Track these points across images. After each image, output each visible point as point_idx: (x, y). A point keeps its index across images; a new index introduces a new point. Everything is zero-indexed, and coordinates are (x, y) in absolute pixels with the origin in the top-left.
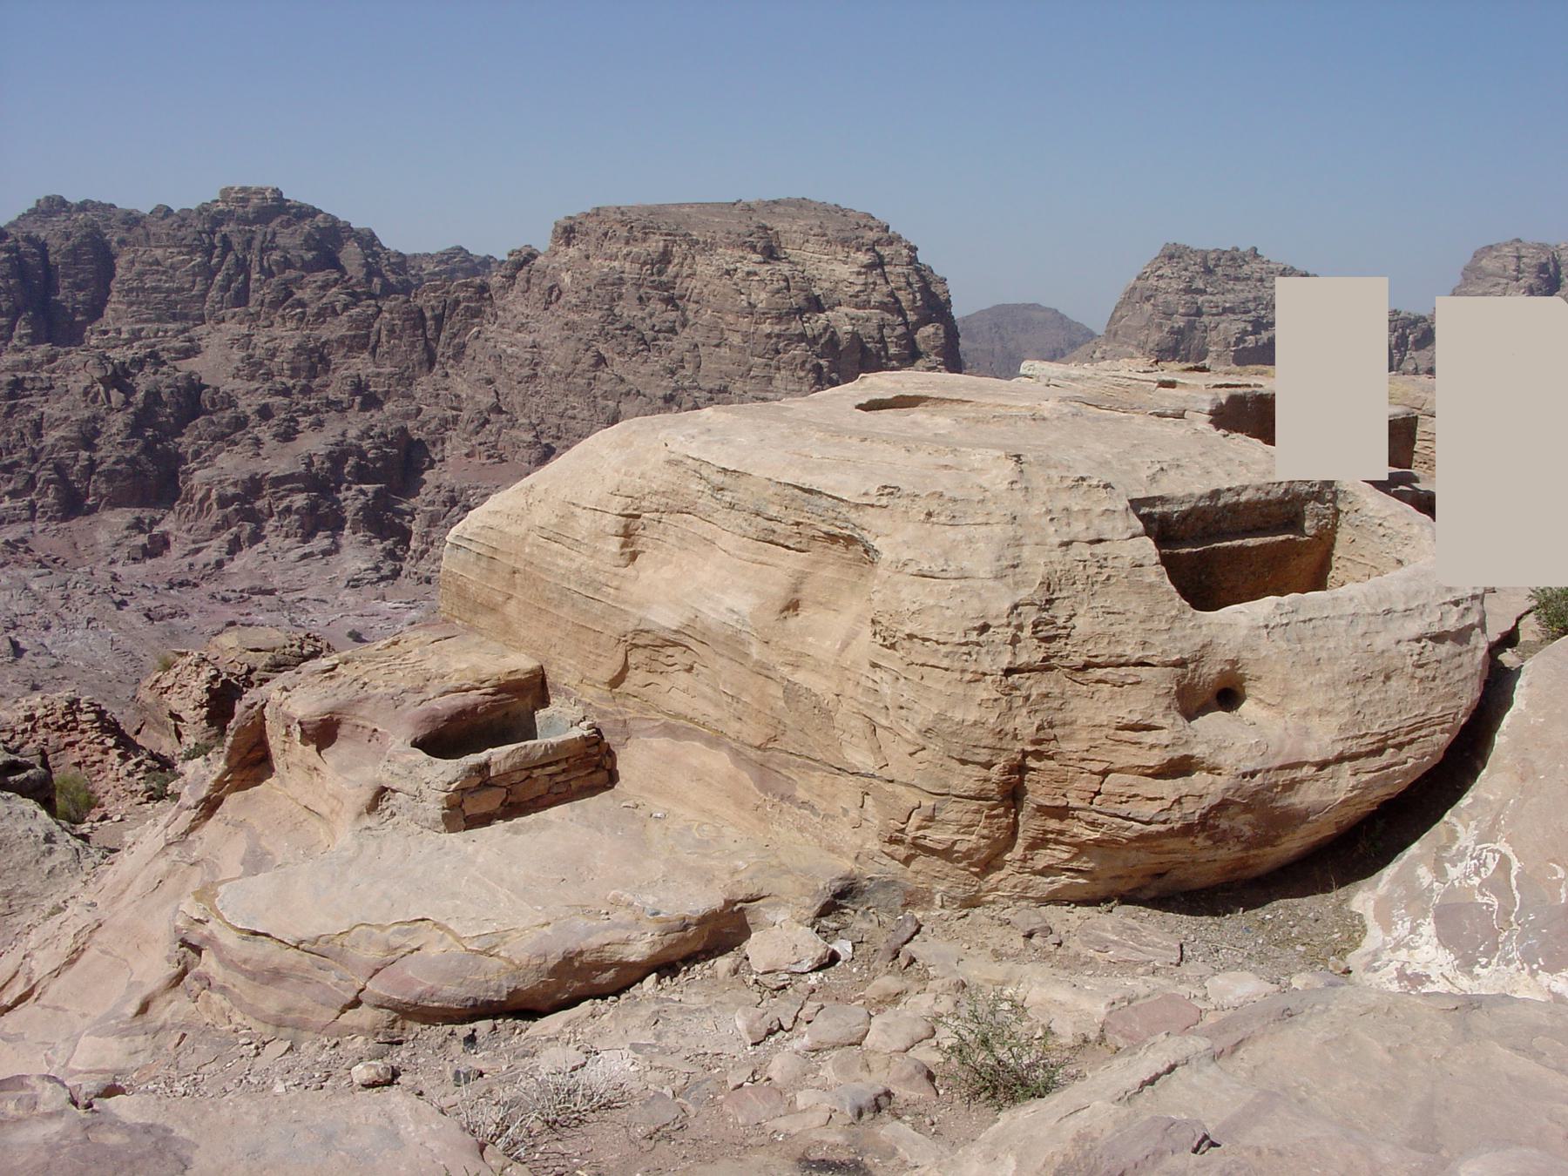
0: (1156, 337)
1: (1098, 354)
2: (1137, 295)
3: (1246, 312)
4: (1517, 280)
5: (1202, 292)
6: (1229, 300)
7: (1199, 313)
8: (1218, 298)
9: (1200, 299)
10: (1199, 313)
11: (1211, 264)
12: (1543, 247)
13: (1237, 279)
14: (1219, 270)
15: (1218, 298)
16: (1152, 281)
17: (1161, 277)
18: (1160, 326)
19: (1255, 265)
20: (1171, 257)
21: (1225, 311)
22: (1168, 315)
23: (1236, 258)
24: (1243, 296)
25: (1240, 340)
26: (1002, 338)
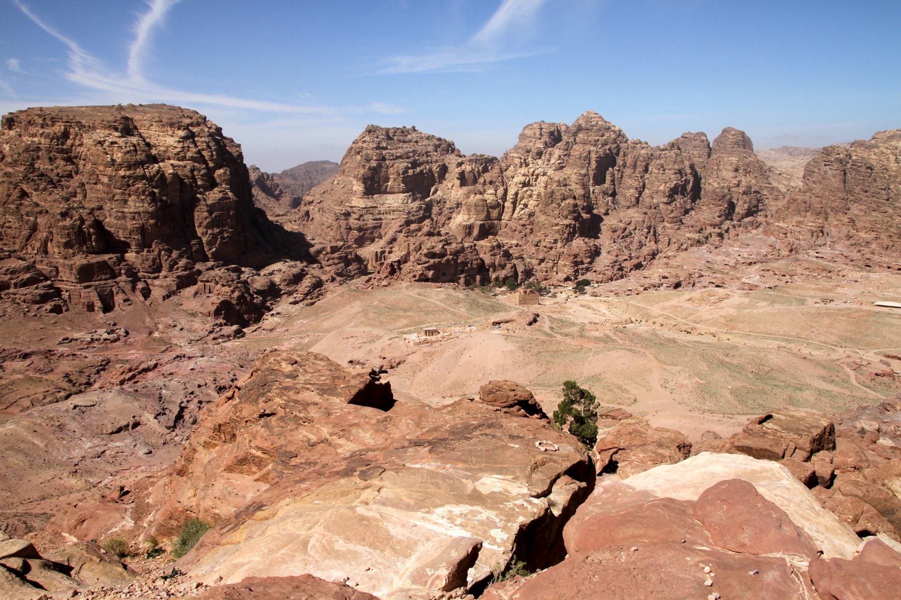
0: (362, 171)
2: (354, 151)
5: (386, 148)
6: (400, 152)
7: (384, 159)
8: (394, 151)
9: (384, 152)
10: (384, 159)
11: (391, 135)
12: (553, 124)
13: (404, 142)
14: (395, 138)
15: (394, 151)
16: (360, 144)
17: (364, 142)
18: (364, 166)
20: (370, 132)
21: (397, 158)
22: (368, 160)
23: (404, 132)
25: (405, 172)
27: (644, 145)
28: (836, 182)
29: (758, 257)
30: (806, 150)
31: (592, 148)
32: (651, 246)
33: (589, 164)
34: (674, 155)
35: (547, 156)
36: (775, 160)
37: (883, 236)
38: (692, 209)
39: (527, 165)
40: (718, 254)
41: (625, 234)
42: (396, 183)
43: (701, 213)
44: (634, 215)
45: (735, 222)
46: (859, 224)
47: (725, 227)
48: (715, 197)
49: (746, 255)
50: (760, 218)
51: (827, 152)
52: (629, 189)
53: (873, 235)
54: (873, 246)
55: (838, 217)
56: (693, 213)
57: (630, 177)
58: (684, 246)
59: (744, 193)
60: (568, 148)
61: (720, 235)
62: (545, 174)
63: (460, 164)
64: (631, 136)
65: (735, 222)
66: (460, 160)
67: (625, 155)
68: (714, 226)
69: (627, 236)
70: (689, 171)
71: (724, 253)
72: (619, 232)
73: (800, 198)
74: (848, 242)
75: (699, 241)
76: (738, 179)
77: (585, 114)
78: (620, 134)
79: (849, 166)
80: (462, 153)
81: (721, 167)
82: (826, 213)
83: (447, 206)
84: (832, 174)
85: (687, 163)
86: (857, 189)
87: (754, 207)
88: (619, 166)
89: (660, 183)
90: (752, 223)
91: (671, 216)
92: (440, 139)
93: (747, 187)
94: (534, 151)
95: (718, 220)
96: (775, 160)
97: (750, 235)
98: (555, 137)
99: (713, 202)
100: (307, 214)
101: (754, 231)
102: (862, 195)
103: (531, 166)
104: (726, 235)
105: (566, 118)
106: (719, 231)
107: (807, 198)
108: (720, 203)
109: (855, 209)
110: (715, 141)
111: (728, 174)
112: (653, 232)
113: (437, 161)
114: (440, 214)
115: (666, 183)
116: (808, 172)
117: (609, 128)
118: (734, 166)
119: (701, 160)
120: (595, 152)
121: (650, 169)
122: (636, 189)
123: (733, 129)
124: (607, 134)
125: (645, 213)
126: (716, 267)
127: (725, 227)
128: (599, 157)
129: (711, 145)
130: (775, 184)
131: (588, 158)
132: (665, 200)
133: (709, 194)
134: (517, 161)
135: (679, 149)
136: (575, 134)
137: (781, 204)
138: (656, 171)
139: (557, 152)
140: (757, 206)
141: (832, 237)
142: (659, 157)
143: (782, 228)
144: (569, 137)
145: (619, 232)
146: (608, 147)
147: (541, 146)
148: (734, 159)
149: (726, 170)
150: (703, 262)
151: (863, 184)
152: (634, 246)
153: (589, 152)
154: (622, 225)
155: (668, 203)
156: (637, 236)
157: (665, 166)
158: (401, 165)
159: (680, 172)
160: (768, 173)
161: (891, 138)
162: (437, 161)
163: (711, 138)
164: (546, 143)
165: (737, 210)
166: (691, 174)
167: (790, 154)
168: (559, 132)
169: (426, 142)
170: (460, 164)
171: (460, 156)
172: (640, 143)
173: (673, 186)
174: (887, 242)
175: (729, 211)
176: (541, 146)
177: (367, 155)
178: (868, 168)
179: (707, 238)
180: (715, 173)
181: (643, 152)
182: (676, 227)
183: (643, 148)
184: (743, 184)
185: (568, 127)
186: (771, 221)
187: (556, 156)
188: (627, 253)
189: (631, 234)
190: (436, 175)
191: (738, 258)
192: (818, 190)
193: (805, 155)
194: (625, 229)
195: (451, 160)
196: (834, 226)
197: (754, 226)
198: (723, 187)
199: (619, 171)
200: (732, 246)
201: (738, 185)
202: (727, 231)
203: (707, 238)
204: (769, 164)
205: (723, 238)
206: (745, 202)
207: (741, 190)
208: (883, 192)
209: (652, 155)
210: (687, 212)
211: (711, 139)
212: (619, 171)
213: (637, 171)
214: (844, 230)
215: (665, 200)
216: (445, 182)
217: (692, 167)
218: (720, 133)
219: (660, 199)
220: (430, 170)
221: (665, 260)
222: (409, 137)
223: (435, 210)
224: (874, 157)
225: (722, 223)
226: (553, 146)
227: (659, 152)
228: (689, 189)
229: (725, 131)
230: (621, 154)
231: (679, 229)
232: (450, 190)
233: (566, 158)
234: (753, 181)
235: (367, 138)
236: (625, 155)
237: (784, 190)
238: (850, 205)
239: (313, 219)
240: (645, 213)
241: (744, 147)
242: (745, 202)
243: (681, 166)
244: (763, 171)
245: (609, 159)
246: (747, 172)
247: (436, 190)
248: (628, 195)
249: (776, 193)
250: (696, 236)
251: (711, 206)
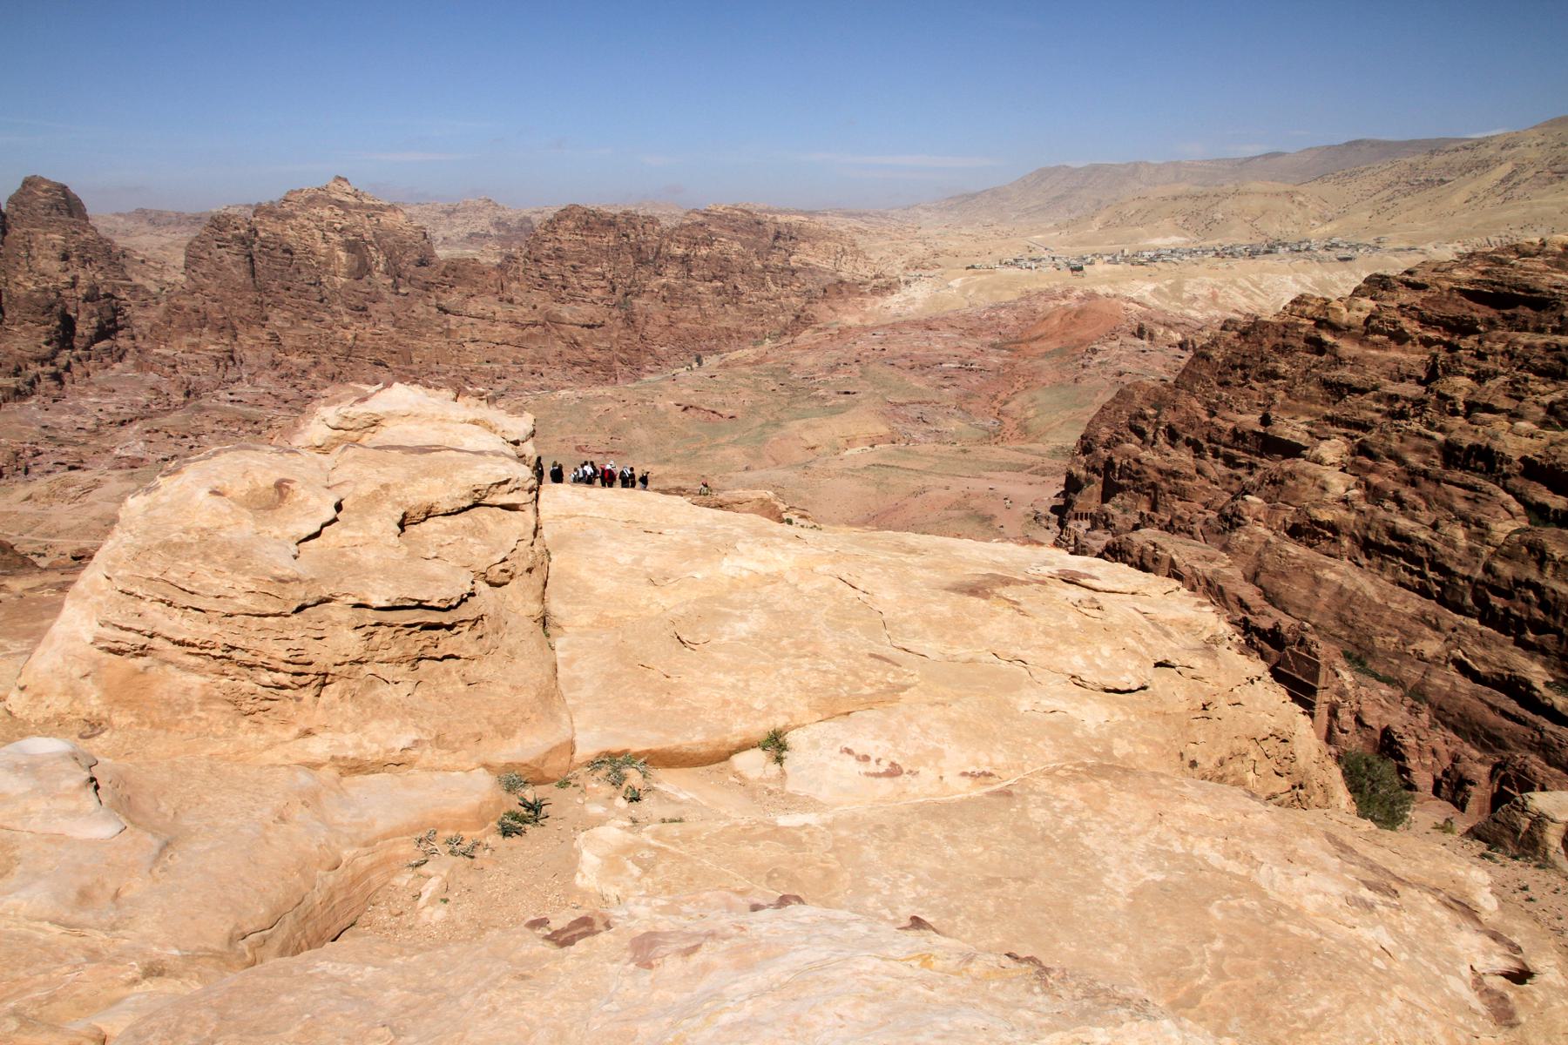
28: (240, 275)
29: (135, 410)
30: (178, 215)
36: (127, 234)
37: (324, 359)
46: (287, 342)
48: (34, 308)
49: (112, 409)
50: (123, 342)
51: (219, 223)
53: (310, 359)
54: (313, 376)
55: (252, 332)
59: (87, 299)
61: (57, 377)
65: (80, 352)
68: (42, 361)
73: (187, 303)
74: (275, 373)
75: (17, 392)
76: (72, 273)
79: (256, 247)
81: (34, 252)
82: (234, 328)
84: (230, 257)
86: (274, 286)
87: (109, 322)
90: (109, 351)
93: (91, 287)
95: (46, 350)
96: (127, 234)
97: (113, 373)
99: (30, 317)
101: (118, 366)
102: (283, 295)
106: (53, 369)
107: (198, 304)
108: (45, 318)
109: (277, 318)
110: (11, 200)
116: (192, 261)
118: (59, 250)
126: (62, 434)
130: (138, 280)
137: (155, 313)
140: (114, 321)
141: (249, 366)
143: (165, 357)
149: (45, 257)
151: (282, 277)
160: (121, 260)
161: (311, 201)
165: (79, 329)
167: (152, 222)
174: (331, 368)
175: (65, 334)
178: (286, 251)
179: (32, 384)
180: (23, 263)
184: (82, 281)
186: (145, 346)
191: (100, 415)
192: (213, 289)
193: (179, 224)
196: (249, 345)
197: (115, 356)
198: (46, 290)
200: (84, 395)
201: (73, 285)
202: (68, 368)
203: (32, 384)
204: (121, 242)
205: (62, 383)
206: (92, 315)
207: (81, 293)
208: (313, 289)
214: (266, 353)
218: (18, 186)
224: (291, 233)
225: (55, 354)
229: (29, 183)
234: (100, 277)
237: (154, 289)
238: (267, 311)
241: (71, 214)
242: (92, 315)
244: (114, 258)
246: (85, 262)
249: (142, 296)
250: (11, 382)
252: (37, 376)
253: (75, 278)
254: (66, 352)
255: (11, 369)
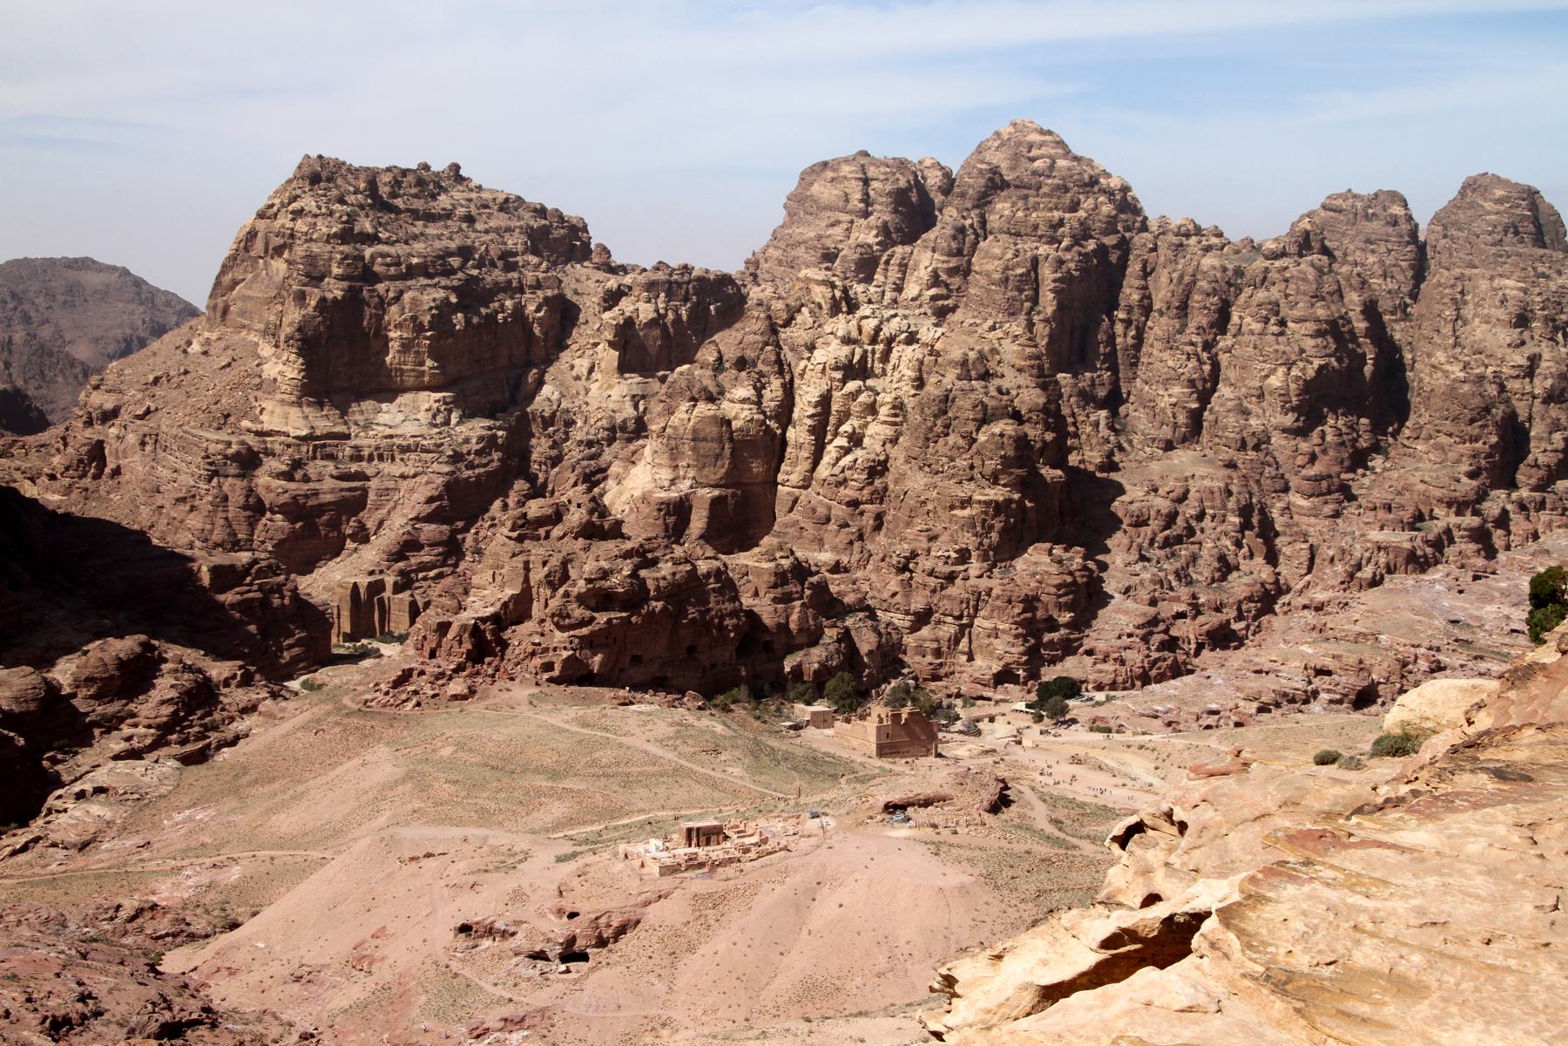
0: (294, 315)
1: (196, 347)
3: (449, 272)
4: (866, 215)
5: (373, 239)
8: (399, 249)
9: (368, 252)
11: (384, 191)
12: (902, 164)
13: (430, 217)
15: (399, 249)
16: (284, 221)
17: (299, 213)
18: (301, 297)
19: (458, 194)
20: (315, 179)
21: (411, 272)
22: (315, 277)
23: (426, 182)
24: (438, 245)
26: (27, 319)
27: (1215, 240)
31: (1043, 250)
32: (1253, 572)
33: (1035, 300)
34: (1311, 274)
35: (894, 274)
38: (1376, 448)
39: (853, 307)
40: (1486, 598)
41: (1176, 532)
42: (411, 358)
43: (1409, 463)
44: (1197, 469)
45: (1524, 493)
47: (1492, 507)
48: (1456, 409)
52: (1167, 382)
56: (1377, 462)
57: (1169, 343)
58: (1367, 573)
60: (963, 246)
61: (1481, 537)
62: (912, 339)
63: (612, 298)
64: (1160, 204)
65: (1524, 493)
66: (612, 283)
67: (1146, 273)
68: (1460, 506)
69: (1179, 540)
70: (1360, 325)
71: (1505, 593)
72: (1155, 524)
77: (1006, 130)
78: (1126, 204)
80: (617, 259)
81: (1468, 312)
83: (578, 434)
85: (1354, 299)
88: (1130, 309)
89: (1266, 370)
91: (1312, 471)
92: (541, 212)
94: (849, 253)
95: (1468, 486)
98: (913, 210)
99: (1448, 426)
100: (97, 452)
103: (865, 310)
104: (1498, 537)
105: (945, 145)
106: (1474, 521)
108: (1474, 430)
110: (1437, 219)
111: (1491, 334)
112: (1259, 527)
113: (538, 285)
114: (556, 461)
115: (1289, 365)
117: (1093, 181)
118: (1513, 308)
119: (1392, 285)
120: (1054, 262)
121: (1235, 318)
122: (1192, 383)
123: (1499, 181)
124: (1088, 204)
125: (1231, 465)
126: (1482, 639)
127: (1492, 507)
128: (1067, 279)
129: (1422, 238)
131: (1031, 279)
132: (1289, 420)
133: (1436, 402)
134: (820, 294)
135: (1325, 251)
136: (983, 201)
138: (1257, 327)
139: (925, 259)
142: (1264, 281)
144: (964, 212)
145: (1155, 524)
146: (1091, 245)
147: (871, 238)
148: (1511, 286)
150: (1439, 623)
152: (1203, 571)
153: (1035, 262)
154: (1162, 504)
155: (1302, 432)
156: (1214, 539)
157: (1284, 311)
158: (427, 296)
159: (1335, 330)
162: (538, 285)
163: (1423, 217)
164: (884, 229)
166: (1369, 333)
168: (920, 186)
169: (499, 220)
170: (612, 298)
171: (613, 270)
172: (1198, 231)
173: (1311, 373)
176: (871, 238)
177: (311, 259)
181: (1209, 261)
182: (1328, 509)
183: (1208, 249)
185: (947, 175)
187: (924, 274)
188: (1184, 592)
189: (1191, 532)
190: (537, 330)
194: (1171, 519)
195: (584, 283)
198: (1481, 378)
199: (1128, 323)
201: (1530, 371)
202: (1503, 521)
207: (1541, 385)
209: (1239, 272)
210: (1359, 460)
211: (1423, 218)
212: (1128, 323)
213: (1192, 326)
215: (1289, 420)
216: (565, 356)
217: (1371, 310)
218: (1453, 192)
219: (1273, 418)
220: (519, 309)
221: (1309, 616)
222: (444, 201)
223: (540, 447)
225: (1482, 496)
226: (910, 238)
227: (1260, 263)
228: (1362, 389)
229: (1474, 187)
230: (1134, 268)
231: (1337, 515)
232: (587, 383)
233: (956, 281)
235: (308, 202)
236: (1146, 273)
239: (117, 472)
240: (1231, 465)
241: (1539, 241)
243: (1335, 310)
245: (1100, 288)
247: (540, 383)
248: (1165, 402)
250: (1402, 539)
251: (1444, 439)
252: (1448, 531)
253: (1534, 360)
254: (1501, 494)
255: (1406, 516)
